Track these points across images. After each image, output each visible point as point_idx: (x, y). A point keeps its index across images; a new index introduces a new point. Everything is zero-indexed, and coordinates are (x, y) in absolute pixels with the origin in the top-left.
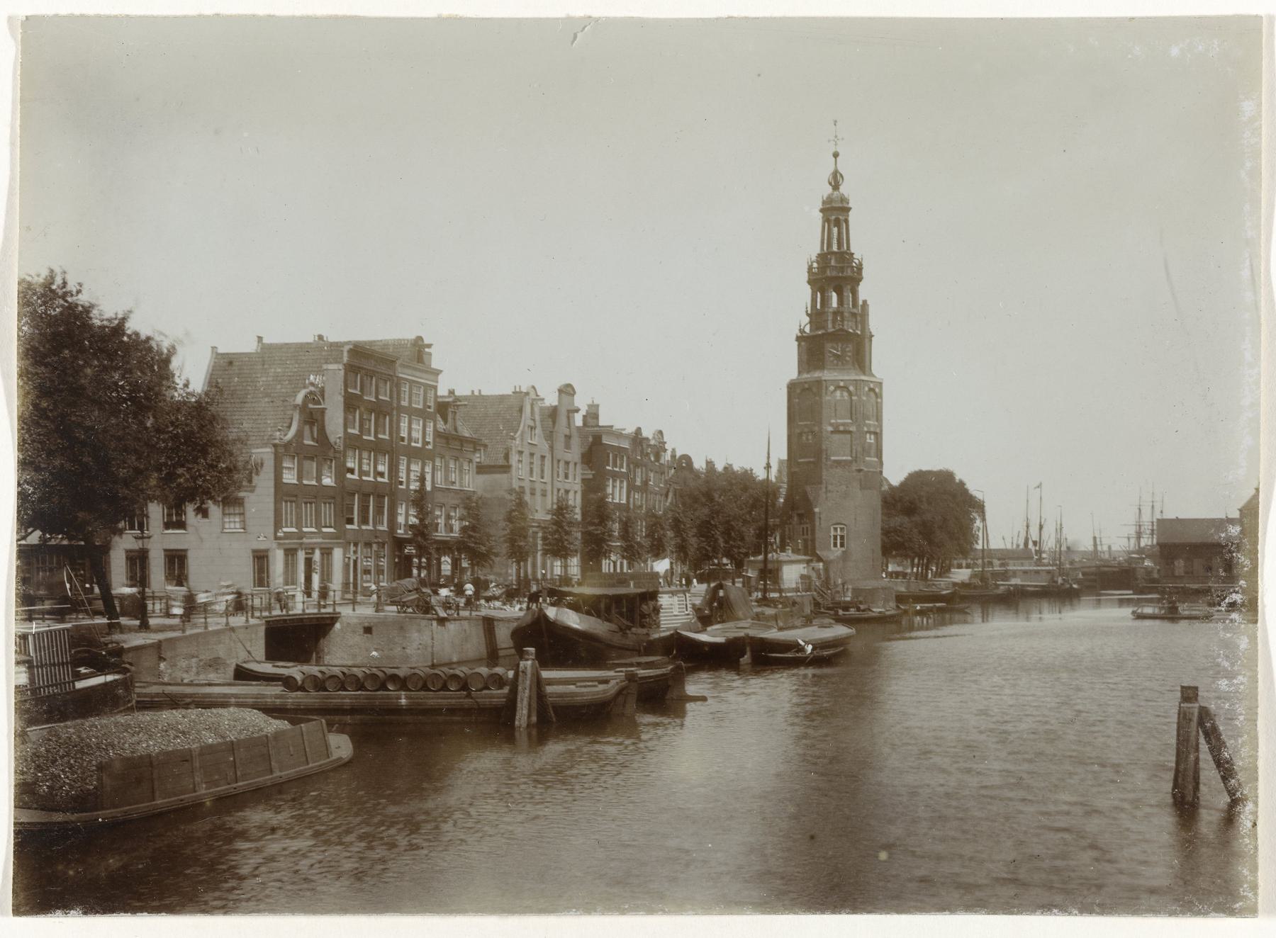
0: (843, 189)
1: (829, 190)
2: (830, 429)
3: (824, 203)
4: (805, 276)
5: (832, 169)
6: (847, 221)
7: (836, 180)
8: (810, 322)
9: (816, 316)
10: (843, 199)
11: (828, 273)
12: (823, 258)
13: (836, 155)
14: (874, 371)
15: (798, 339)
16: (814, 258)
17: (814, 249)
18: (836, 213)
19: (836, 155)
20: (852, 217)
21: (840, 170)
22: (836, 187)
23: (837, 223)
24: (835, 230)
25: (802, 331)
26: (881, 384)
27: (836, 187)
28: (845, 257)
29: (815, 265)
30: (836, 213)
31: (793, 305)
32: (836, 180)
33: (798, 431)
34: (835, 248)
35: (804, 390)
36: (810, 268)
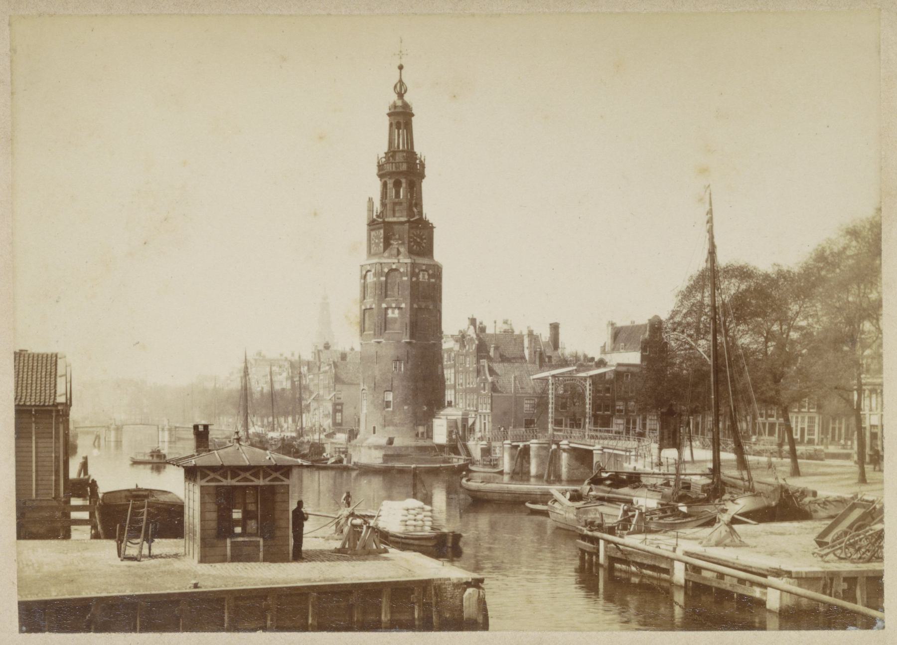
0: (407, 97)
1: (395, 97)
2: (415, 306)
4: (375, 170)
5: (397, 80)
12: (392, 153)
13: (401, 68)
17: (383, 148)
18: (401, 118)
19: (401, 68)
20: (417, 123)
22: (401, 96)
27: (401, 96)
28: (411, 155)
30: (401, 118)
33: (384, 306)
35: (392, 270)
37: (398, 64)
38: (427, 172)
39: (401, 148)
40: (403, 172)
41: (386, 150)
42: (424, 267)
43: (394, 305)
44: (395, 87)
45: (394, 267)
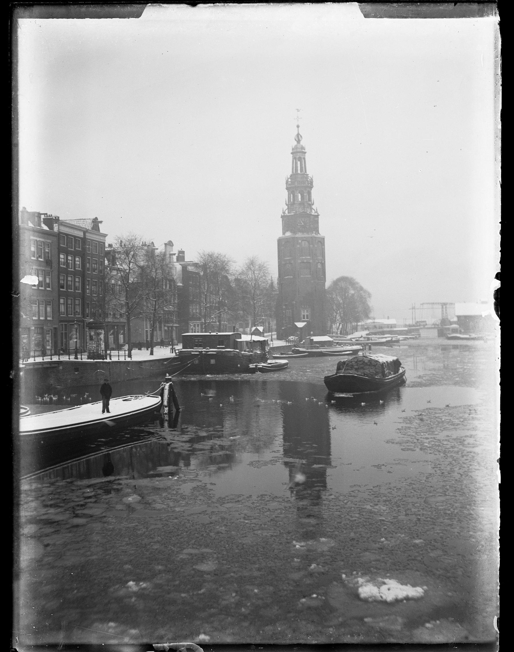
0: (302, 143)
1: (295, 143)
3: (293, 149)
5: (296, 133)
6: (304, 159)
8: (288, 208)
9: (291, 205)
10: (303, 148)
11: (296, 184)
13: (298, 127)
14: (320, 233)
15: (282, 217)
16: (289, 177)
18: (299, 155)
19: (298, 127)
20: (307, 156)
21: (300, 133)
22: (299, 141)
23: (300, 159)
24: (299, 163)
25: (284, 213)
26: (324, 239)
27: (299, 141)
28: (305, 175)
29: (290, 180)
30: (299, 155)
31: (279, 201)
34: (299, 172)
36: (287, 182)
37: (297, 124)
38: (314, 184)
39: (299, 172)
40: (300, 185)
41: (291, 173)
42: (305, 239)
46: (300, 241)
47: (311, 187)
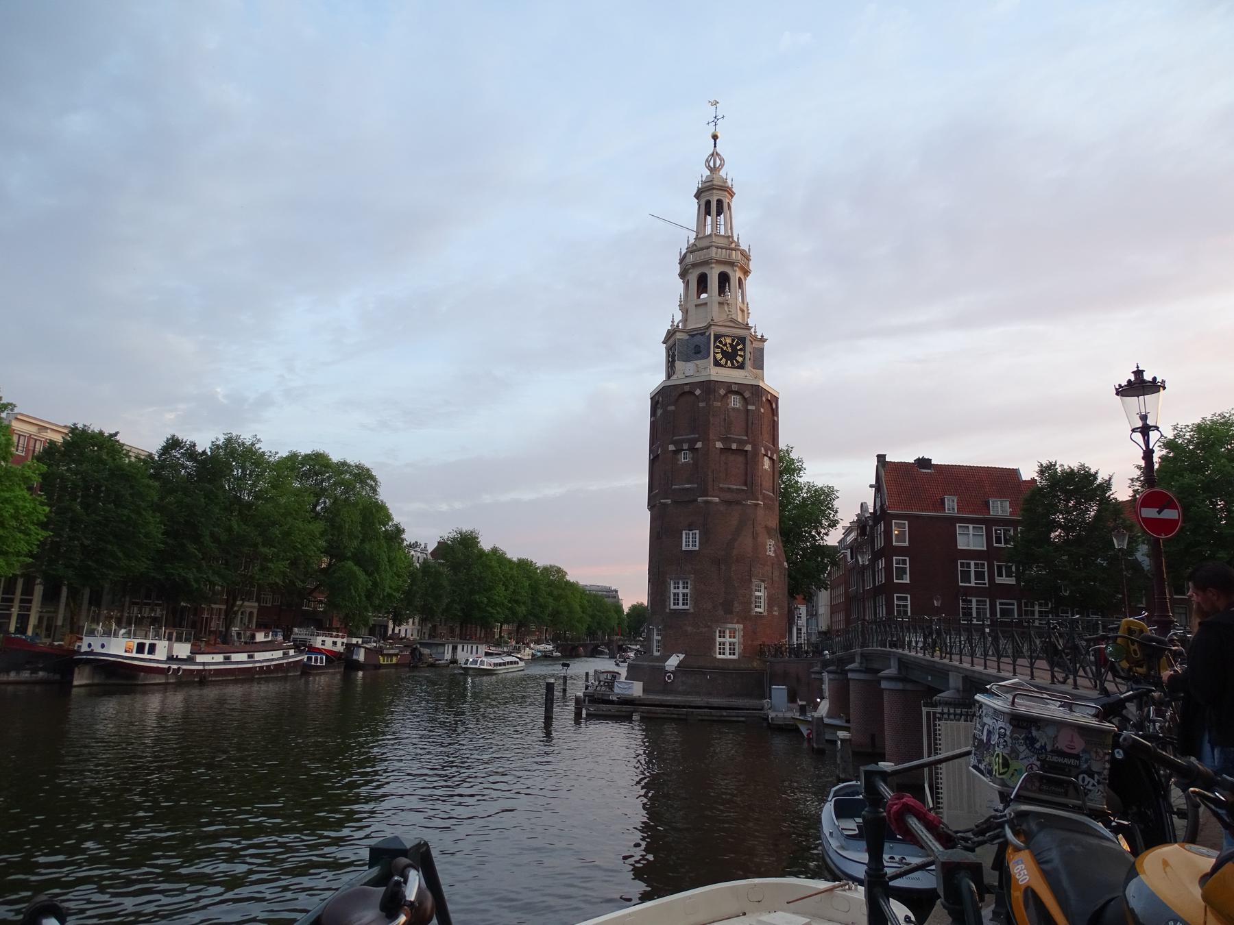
0: (722, 173)
1: (708, 173)
2: (719, 445)
7: (714, 162)
13: (715, 137)
18: (713, 198)
19: (715, 137)
20: (735, 203)
22: (713, 170)
28: (730, 243)
30: (713, 198)
31: (664, 302)
32: (714, 162)
33: (672, 448)
37: (711, 130)
38: (752, 266)
42: (734, 388)
43: (685, 446)
44: (707, 161)
45: (687, 389)
46: (722, 392)
47: (746, 272)
